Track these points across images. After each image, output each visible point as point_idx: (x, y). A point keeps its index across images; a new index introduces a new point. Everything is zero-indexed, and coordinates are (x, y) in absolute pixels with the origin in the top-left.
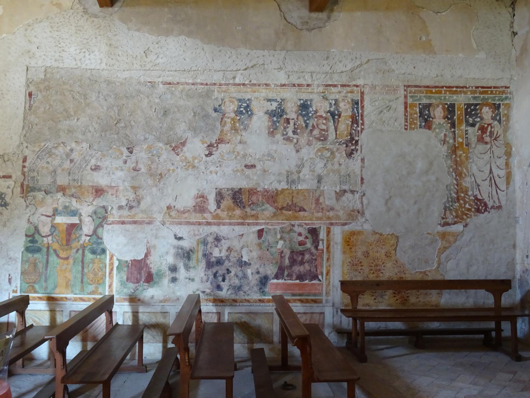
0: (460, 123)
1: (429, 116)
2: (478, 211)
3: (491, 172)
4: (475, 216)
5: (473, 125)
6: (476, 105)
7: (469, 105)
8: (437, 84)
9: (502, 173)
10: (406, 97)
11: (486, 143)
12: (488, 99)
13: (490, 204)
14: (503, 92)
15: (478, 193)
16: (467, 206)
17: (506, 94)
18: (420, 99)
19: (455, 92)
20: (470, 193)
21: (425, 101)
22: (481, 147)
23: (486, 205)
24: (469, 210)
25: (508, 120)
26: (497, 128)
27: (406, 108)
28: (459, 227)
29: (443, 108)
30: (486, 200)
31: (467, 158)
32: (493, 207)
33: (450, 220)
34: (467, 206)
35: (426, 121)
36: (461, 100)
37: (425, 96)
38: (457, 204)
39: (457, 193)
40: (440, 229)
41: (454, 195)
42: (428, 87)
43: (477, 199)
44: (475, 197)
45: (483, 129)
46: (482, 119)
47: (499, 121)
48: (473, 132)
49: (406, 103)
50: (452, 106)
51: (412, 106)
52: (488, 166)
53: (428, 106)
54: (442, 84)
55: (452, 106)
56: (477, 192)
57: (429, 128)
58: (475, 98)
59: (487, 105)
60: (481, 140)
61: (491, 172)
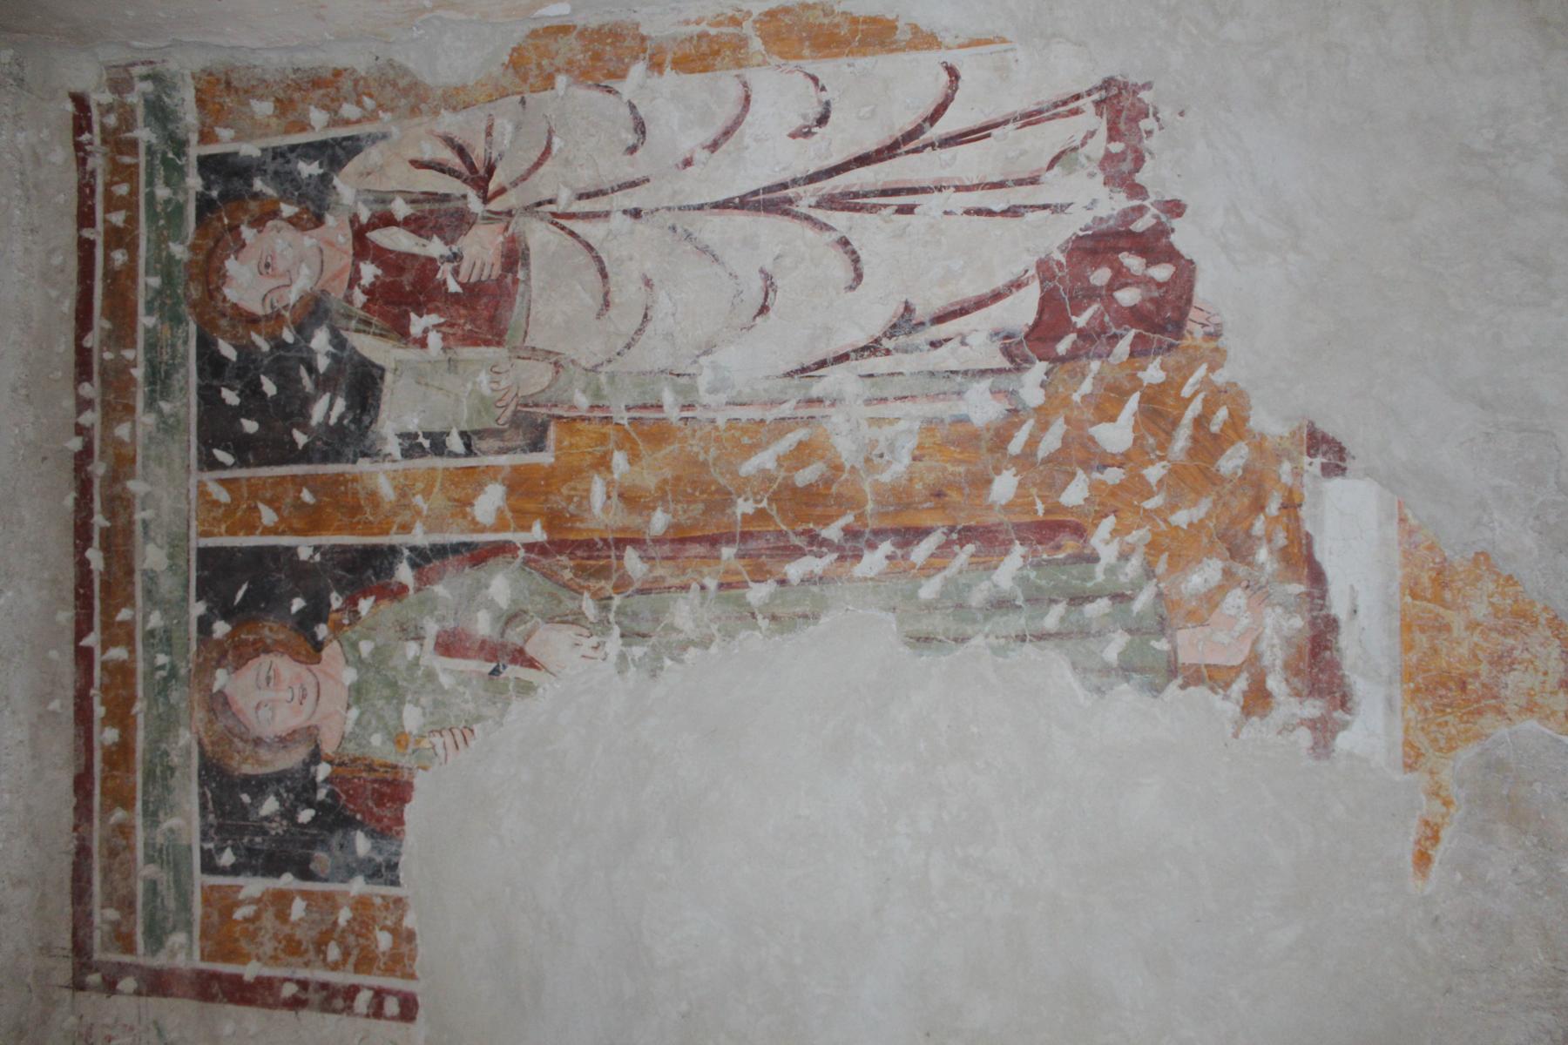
0: (343, 503)
1: (300, 787)
2: (1164, 319)
3: (770, 201)
4: (1217, 359)
5: (363, 386)
6: (211, 364)
7: (216, 429)
8: (62, 704)
9: (779, 93)
10: (158, 984)
11: (514, 256)
12: (167, 267)
13: (1091, 201)
14: (119, 143)
15: (977, 326)
16: (1116, 435)
17: (127, 121)
18: (168, 856)
19: (119, 546)
20: (981, 406)
21: (186, 818)
22: (553, 305)
23: (1099, 245)
24: (1158, 413)
25: (325, 85)
26: (391, 168)
27: (242, 993)
28: (1352, 529)
29: (239, 653)
30: (1051, 237)
31: (649, 432)
32: (1122, 172)
33: (1280, 627)
34: (1116, 435)
35: (335, 818)
36: (175, 499)
37: (152, 817)
38: (1103, 540)
39: (989, 539)
40: (1373, 728)
41: (1011, 567)
42: (82, 784)
43: (1045, 331)
44: (1019, 350)
45: (402, 294)
46: (314, 310)
47: (336, 153)
48: (429, 378)
49: (208, 988)
50: (217, 571)
51: (224, 939)
52: (714, 228)
53: (225, 789)
54: (63, 659)
55: (217, 571)
56: (976, 340)
57: (393, 791)
58: (160, 380)
59: (209, 271)
60: (484, 312)
61: (770, 201)
